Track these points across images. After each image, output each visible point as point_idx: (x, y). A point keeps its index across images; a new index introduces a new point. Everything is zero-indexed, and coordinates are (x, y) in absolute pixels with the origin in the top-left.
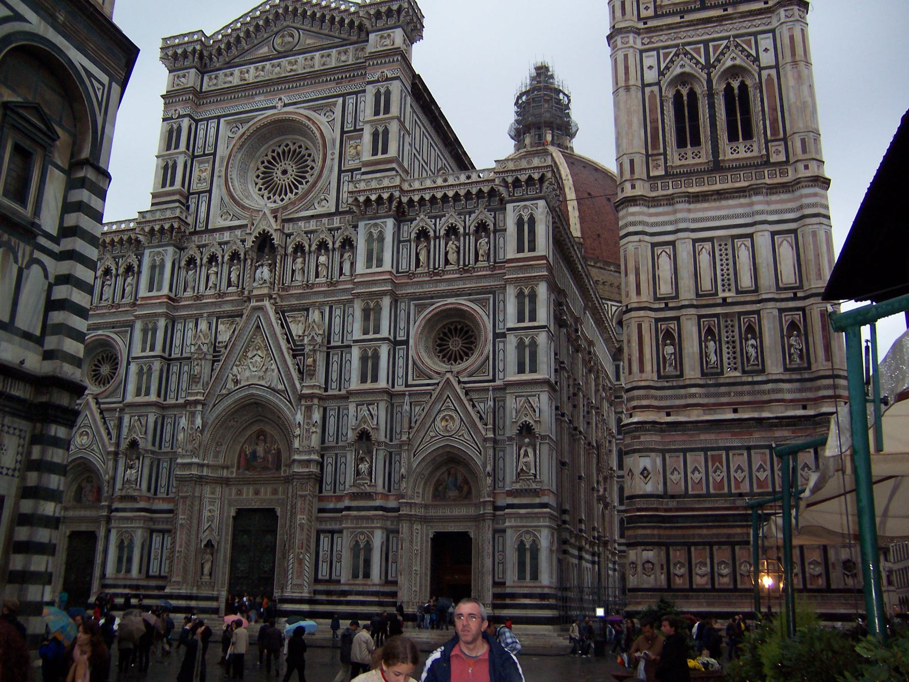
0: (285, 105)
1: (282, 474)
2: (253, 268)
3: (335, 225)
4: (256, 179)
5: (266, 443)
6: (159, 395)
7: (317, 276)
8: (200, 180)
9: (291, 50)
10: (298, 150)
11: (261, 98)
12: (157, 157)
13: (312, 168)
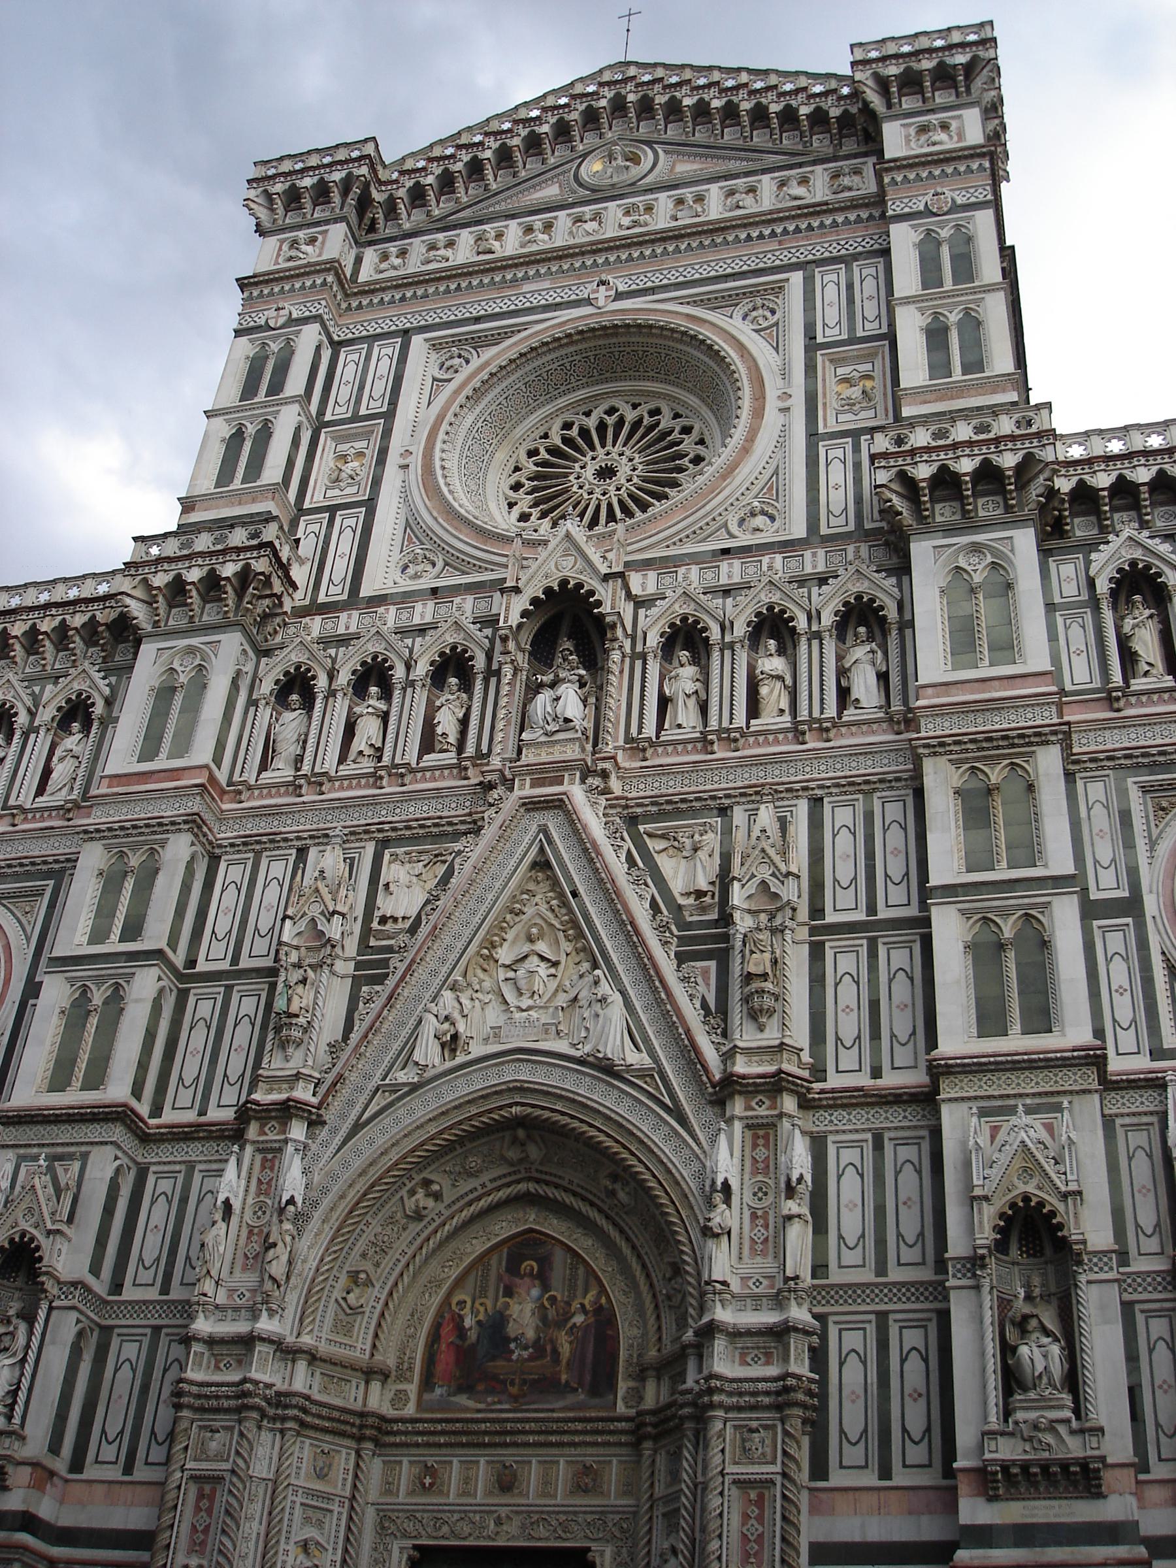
0: (619, 296)
1: (621, 1408)
2: (519, 688)
3: (809, 570)
4: (511, 493)
5: (546, 1287)
6: (137, 1092)
7: (754, 710)
8: (337, 480)
9: (633, 184)
12: (209, 414)
13: (697, 460)
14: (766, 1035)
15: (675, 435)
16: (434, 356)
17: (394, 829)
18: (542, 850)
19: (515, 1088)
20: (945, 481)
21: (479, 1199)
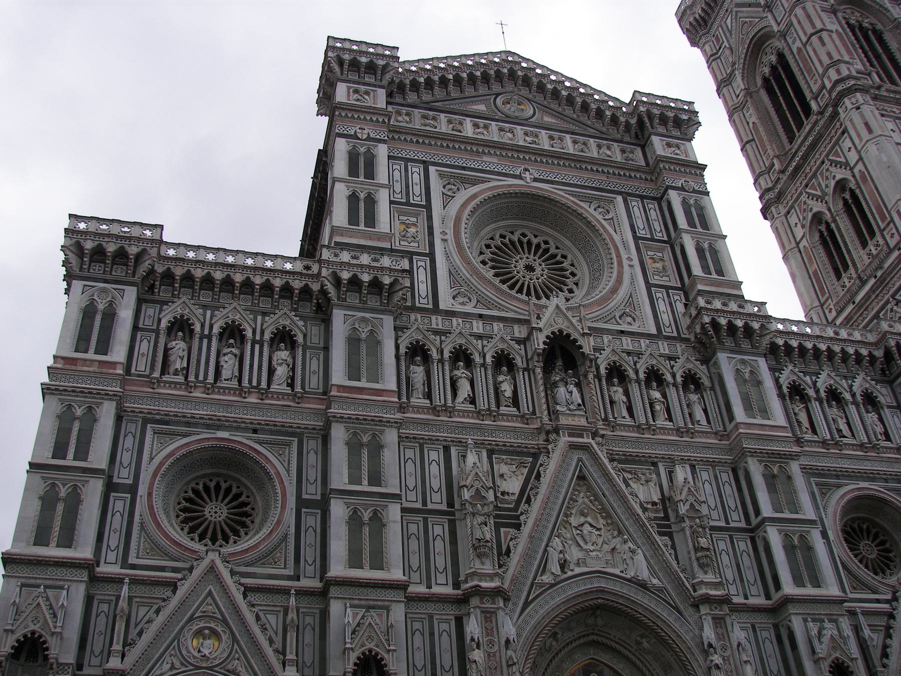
0: (535, 180)
8: (404, 236)
9: (525, 120)
10: (543, 246)
11: (495, 160)
14: (706, 576)
15: (559, 258)
16: (441, 181)
17: (497, 445)
18: (580, 470)
19: (600, 590)
20: (731, 327)
21: (571, 642)
